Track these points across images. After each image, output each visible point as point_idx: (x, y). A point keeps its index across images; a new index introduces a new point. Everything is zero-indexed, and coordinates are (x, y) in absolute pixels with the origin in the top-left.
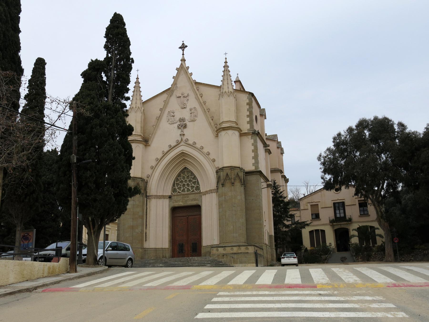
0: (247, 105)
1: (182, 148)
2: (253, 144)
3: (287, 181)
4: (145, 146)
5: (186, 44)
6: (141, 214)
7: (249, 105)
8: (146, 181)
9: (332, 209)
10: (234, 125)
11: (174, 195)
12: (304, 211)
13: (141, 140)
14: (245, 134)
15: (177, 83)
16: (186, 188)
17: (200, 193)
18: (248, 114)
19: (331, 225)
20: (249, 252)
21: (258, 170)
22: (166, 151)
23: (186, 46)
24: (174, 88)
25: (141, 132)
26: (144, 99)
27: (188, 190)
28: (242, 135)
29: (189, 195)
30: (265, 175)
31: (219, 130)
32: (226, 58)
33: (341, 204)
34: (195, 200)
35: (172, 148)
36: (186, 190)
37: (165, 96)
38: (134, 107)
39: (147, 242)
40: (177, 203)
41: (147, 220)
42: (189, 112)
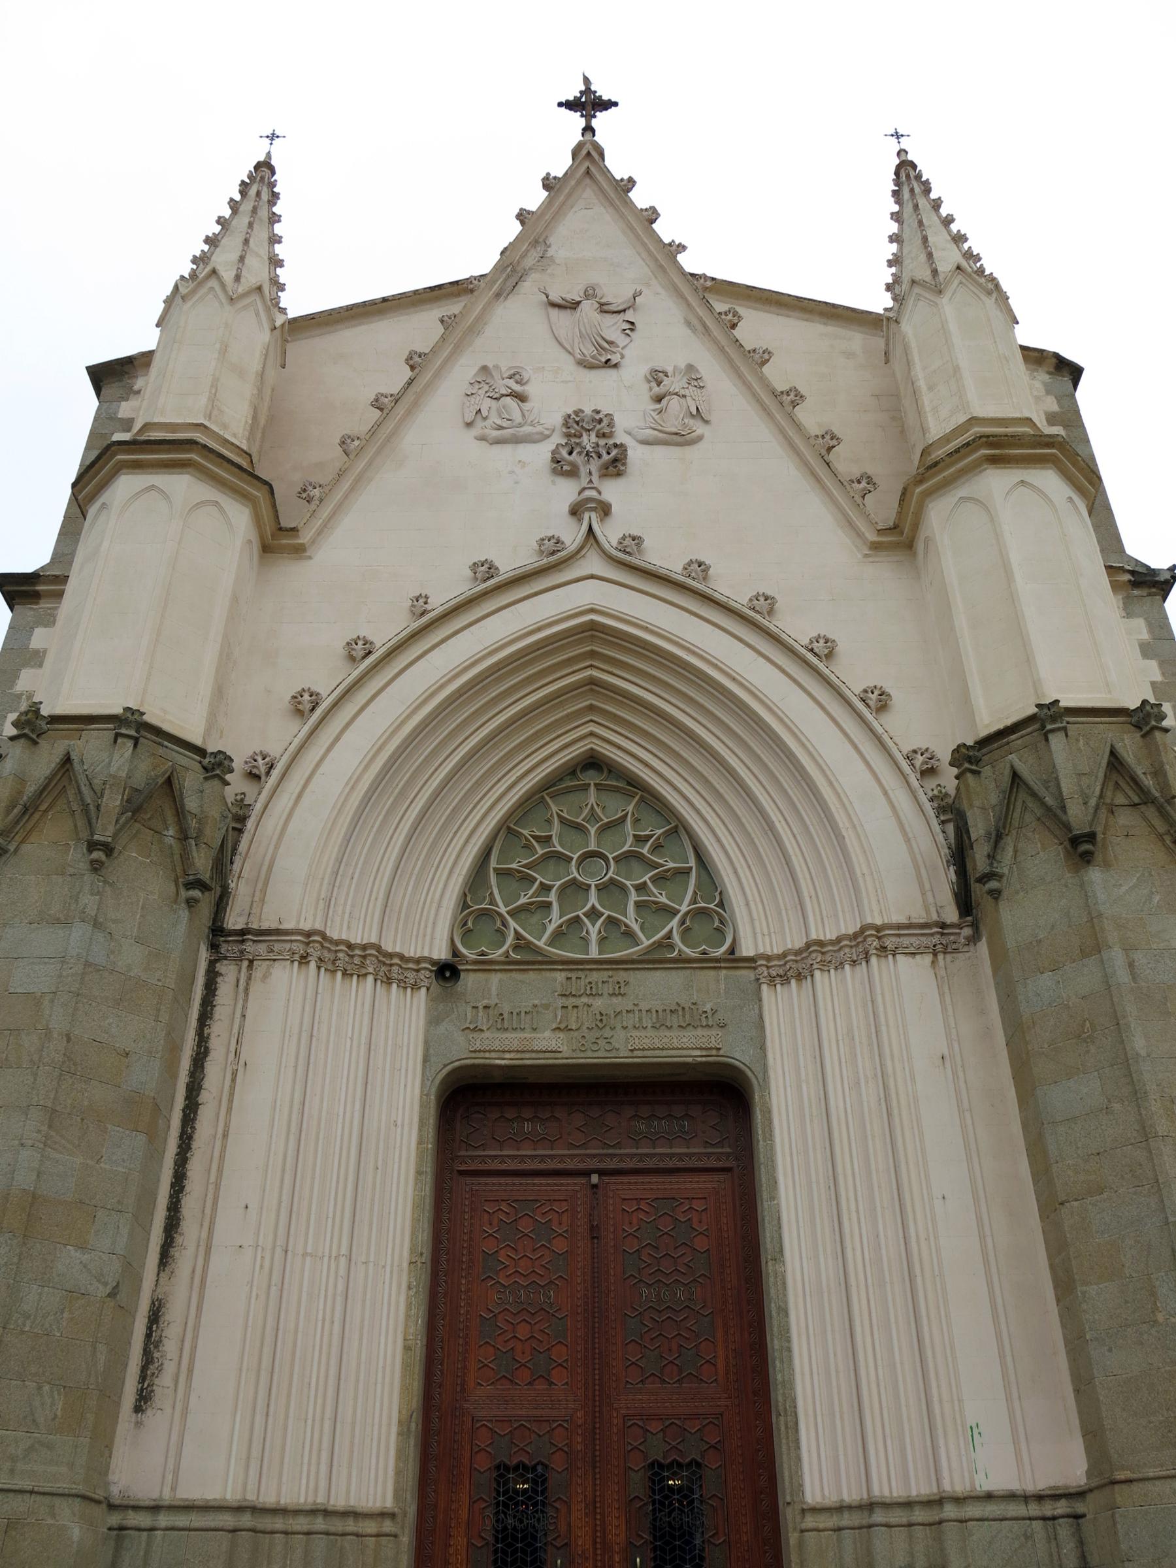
6: (143, 1076)
15: (551, 240)
17: (733, 959)
24: (529, 262)
35: (492, 587)
38: (228, 275)
39: (157, 1419)
40: (512, 1039)
41: (195, 1168)
42: (644, 392)
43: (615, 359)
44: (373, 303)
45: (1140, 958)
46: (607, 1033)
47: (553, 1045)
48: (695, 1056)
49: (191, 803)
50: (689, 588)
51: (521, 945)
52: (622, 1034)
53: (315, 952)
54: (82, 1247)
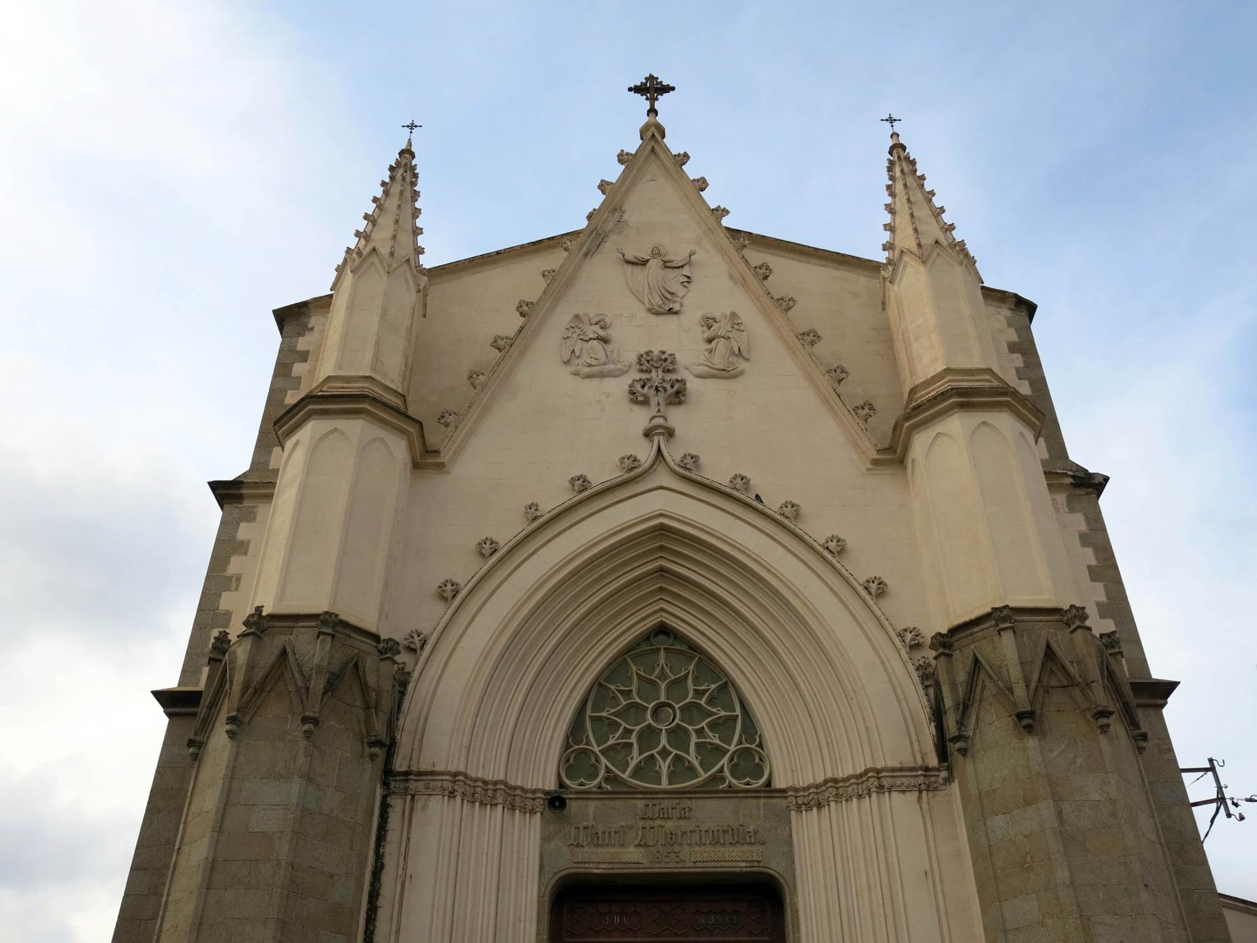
7: (1023, 354)
15: (625, 207)
22: (548, 505)
24: (611, 225)
34: (738, 836)
35: (587, 496)
38: (384, 250)
42: (700, 334)
43: (677, 307)
44: (489, 255)
45: (1066, 807)
46: (677, 848)
47: (636, 858)
48: (742, 867)
49: (371, 680)
50: (738, 496)
51: (611, 778)
52: (687, 848)
53: (460, 789)
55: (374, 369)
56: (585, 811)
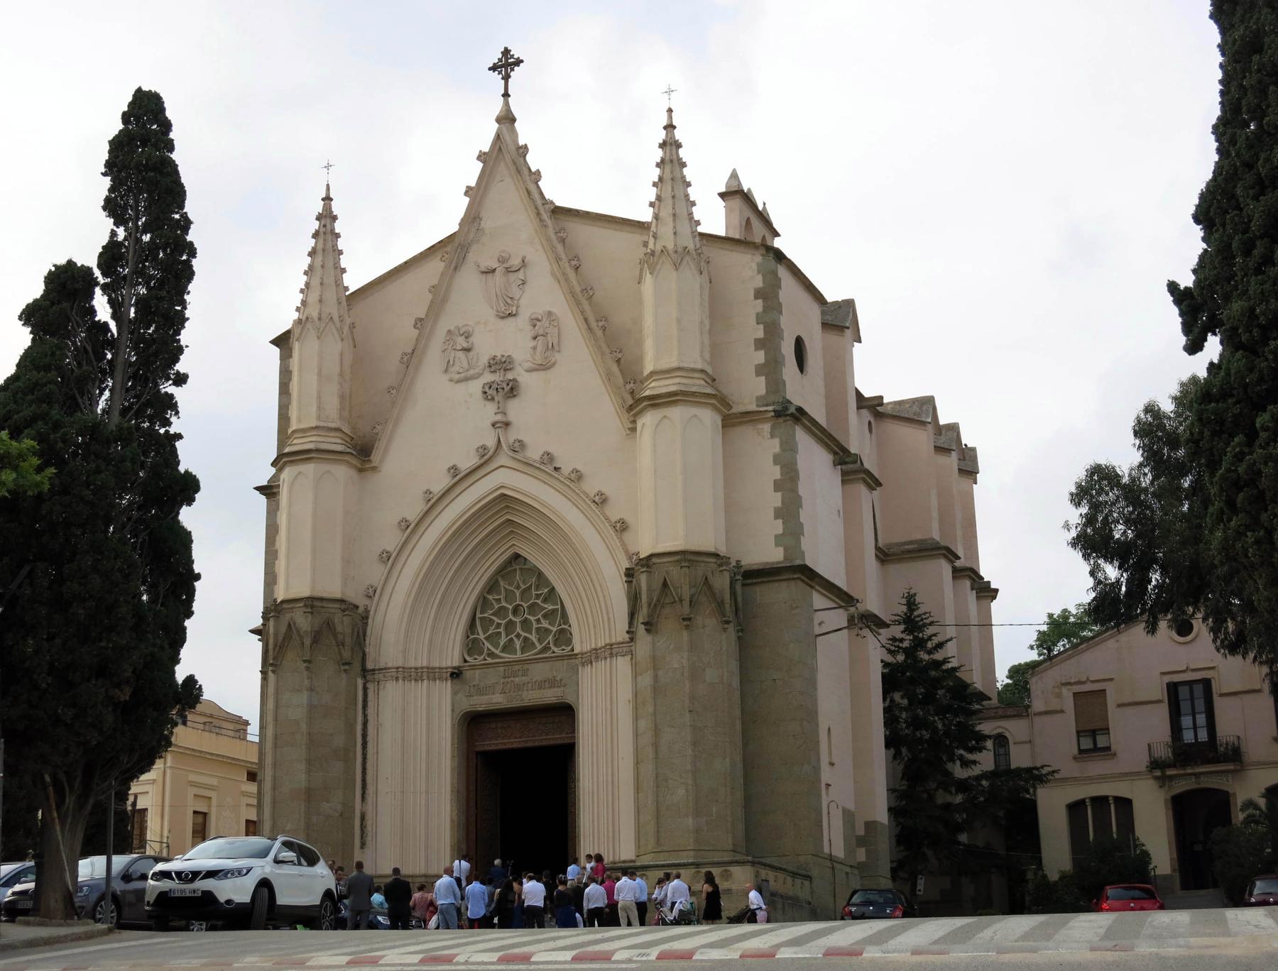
0: (756, 298)
1: (504, 478)
2: (777, 459)
3: (987, 592)
4: (360, 470)
5: (516, 53)
6: (339, 741)
8: (361, 610)
9: (1163, 711)
10: (698, 385)
11: (473, 667)
12: (1046, 718)
13: (339, 448)
14: (748, 418)
16: (518, 636)
17: (572, 656)
18: (760, 334)
19: (1156, 778)
20: (734, 887)
21: (798, 562)
22: (438, 487)
23: (519, 62)
24: (471, 236)
25: (341, 418)
26: (353, 281)
27: (527, 645)
28: (732, 420)
29: (531, 667)
30: (840, 582)
31: (637, 403)
32: (670, 111)
33: (1198, 690)
34: (553, 683)
35: (461, 478)
36: (518, 643)
37: (436, 267)
40: (485, 699)
44: (400, 266)
45: (660, 673)
47: (500, 700)
48: (553, 700)
49: (339, 629)
50: (548, 465)
53: (400, 676)
54: (328, 801)
55: (319, 418)
56: (473, 676)
